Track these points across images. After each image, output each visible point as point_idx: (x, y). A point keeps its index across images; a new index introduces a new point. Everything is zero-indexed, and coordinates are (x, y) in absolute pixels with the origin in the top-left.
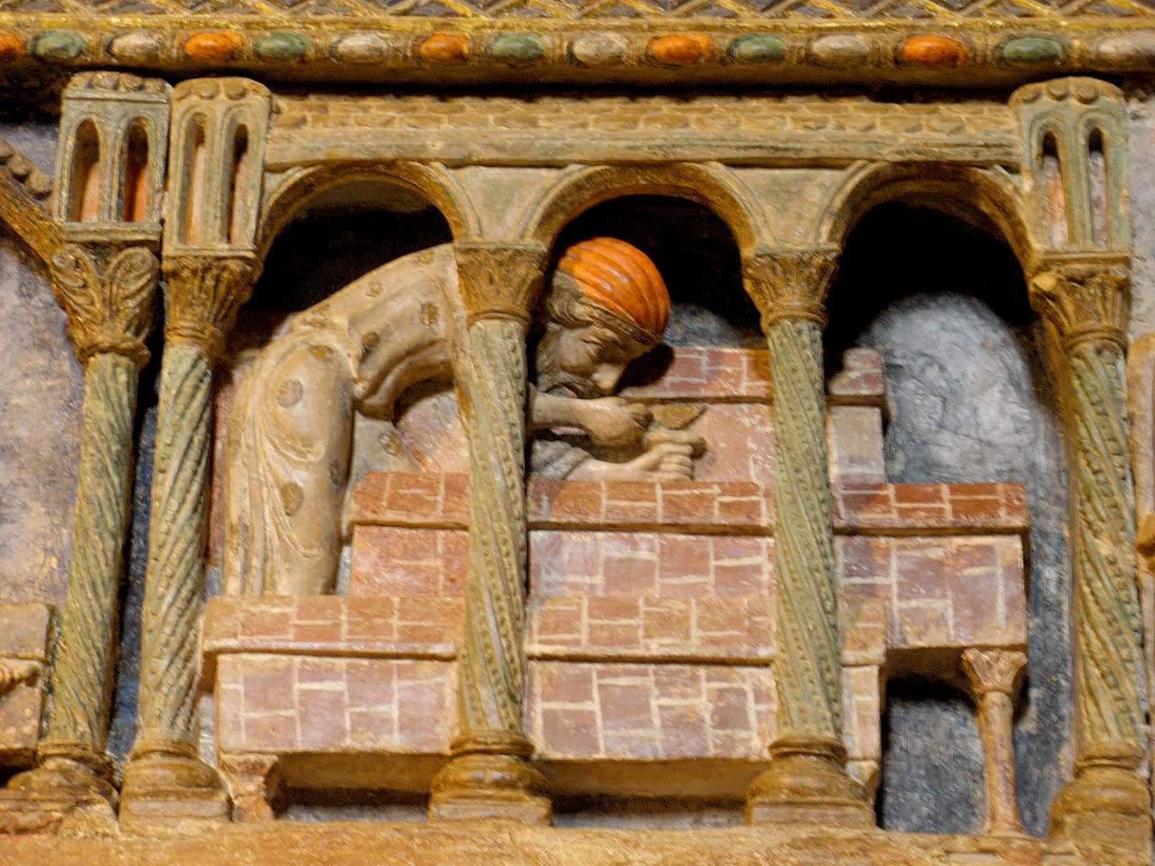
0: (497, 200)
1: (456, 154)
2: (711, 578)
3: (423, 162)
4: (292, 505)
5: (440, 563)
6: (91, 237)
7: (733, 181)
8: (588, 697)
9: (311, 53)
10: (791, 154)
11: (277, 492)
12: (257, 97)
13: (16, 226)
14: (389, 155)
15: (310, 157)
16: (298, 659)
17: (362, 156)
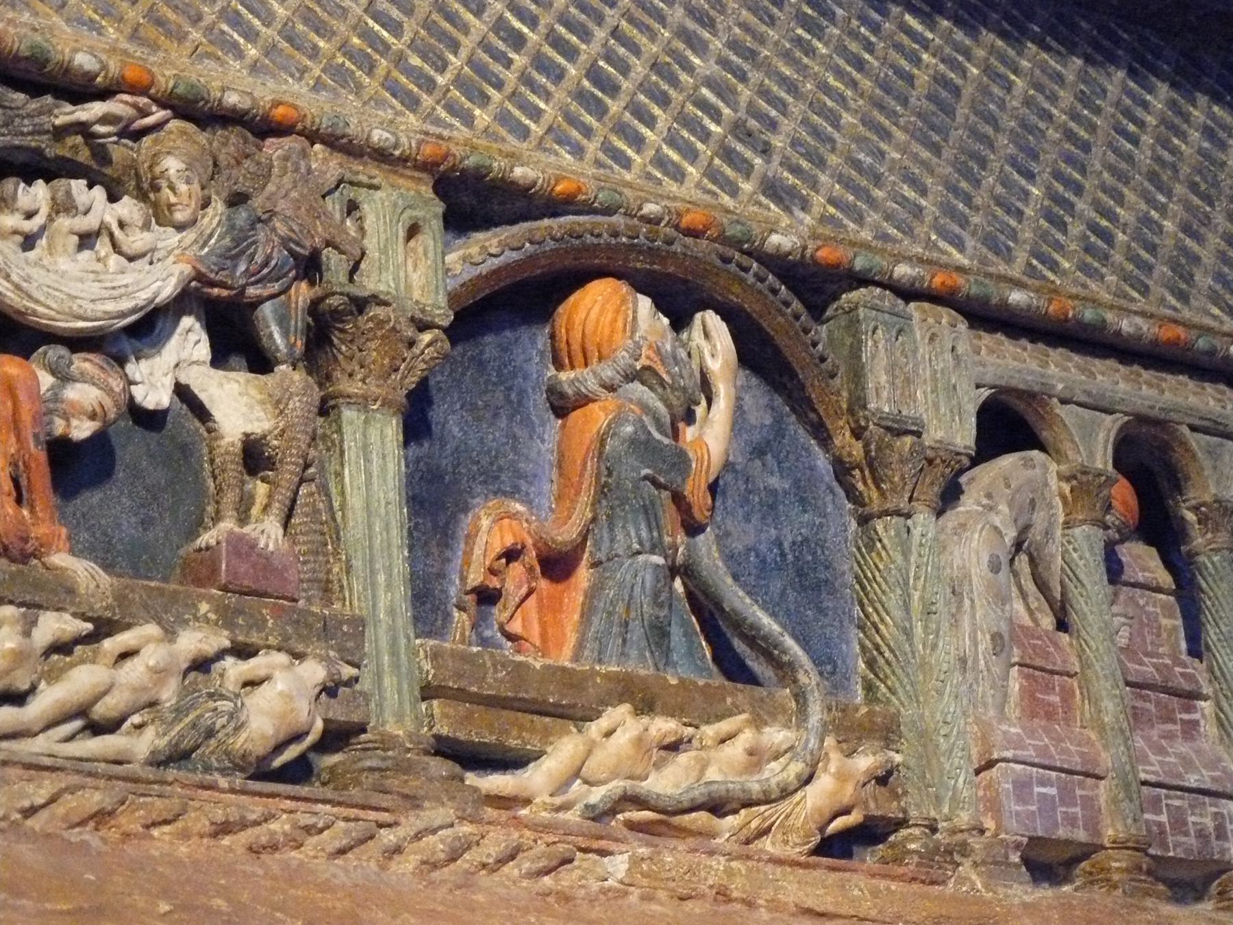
0: (1088, 433)
1: (1068, 395)
2: (1178, 727)
3: (1050, 397)
4: (998, 649)
5: (1058, 699)
6: (890, 424)
7: (1196, 441)
8: (1161, 812)
9: (994, 301)
10: (1221, 428)
11: (988, 637)
12: (963, 326)
13: (813, 396)
14: (1036, 388)
15: (998, 383)
16: (1035, 769)
17: (1021, 386)
